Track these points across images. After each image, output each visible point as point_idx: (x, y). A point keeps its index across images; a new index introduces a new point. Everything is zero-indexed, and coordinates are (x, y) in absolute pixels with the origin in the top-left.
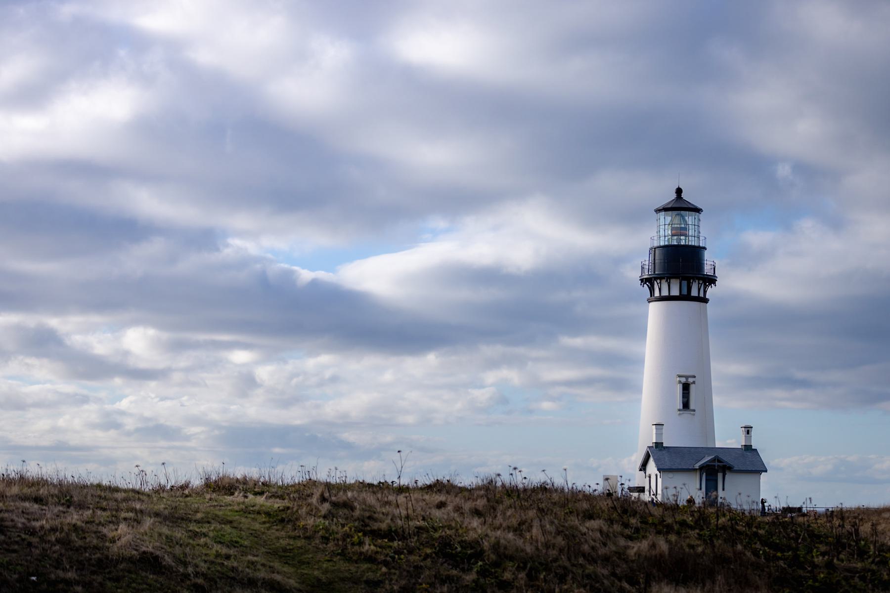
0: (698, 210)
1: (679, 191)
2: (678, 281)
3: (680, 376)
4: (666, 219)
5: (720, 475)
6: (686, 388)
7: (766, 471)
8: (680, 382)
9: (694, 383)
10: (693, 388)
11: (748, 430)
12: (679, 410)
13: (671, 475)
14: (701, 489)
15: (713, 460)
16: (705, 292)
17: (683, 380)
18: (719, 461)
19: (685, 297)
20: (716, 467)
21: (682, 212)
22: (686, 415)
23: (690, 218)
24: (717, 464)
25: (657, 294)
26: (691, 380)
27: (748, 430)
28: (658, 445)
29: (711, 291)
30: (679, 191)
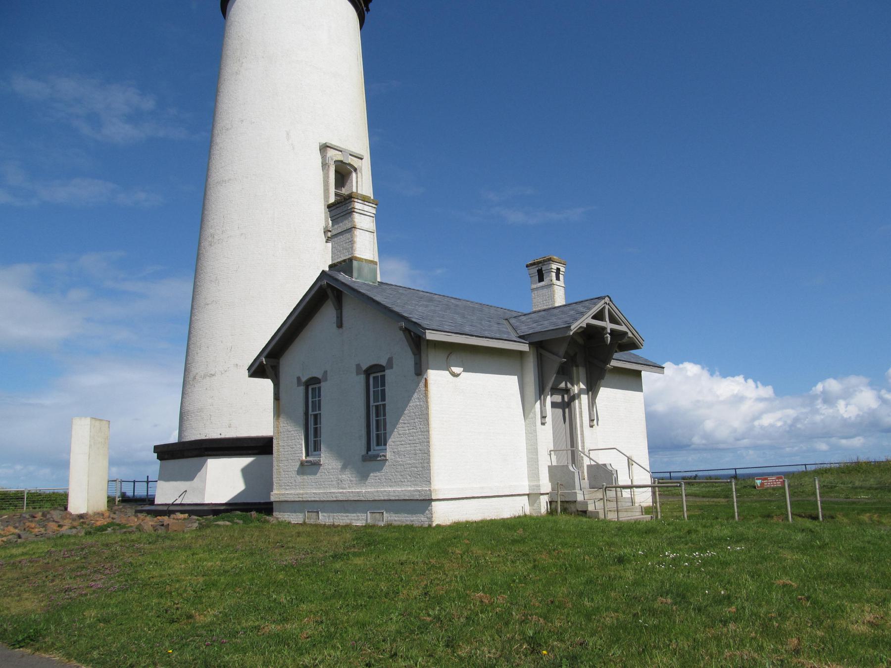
3: (324, 148)
14: (544, 417)
15: (599, 316)
24: (609, 326)
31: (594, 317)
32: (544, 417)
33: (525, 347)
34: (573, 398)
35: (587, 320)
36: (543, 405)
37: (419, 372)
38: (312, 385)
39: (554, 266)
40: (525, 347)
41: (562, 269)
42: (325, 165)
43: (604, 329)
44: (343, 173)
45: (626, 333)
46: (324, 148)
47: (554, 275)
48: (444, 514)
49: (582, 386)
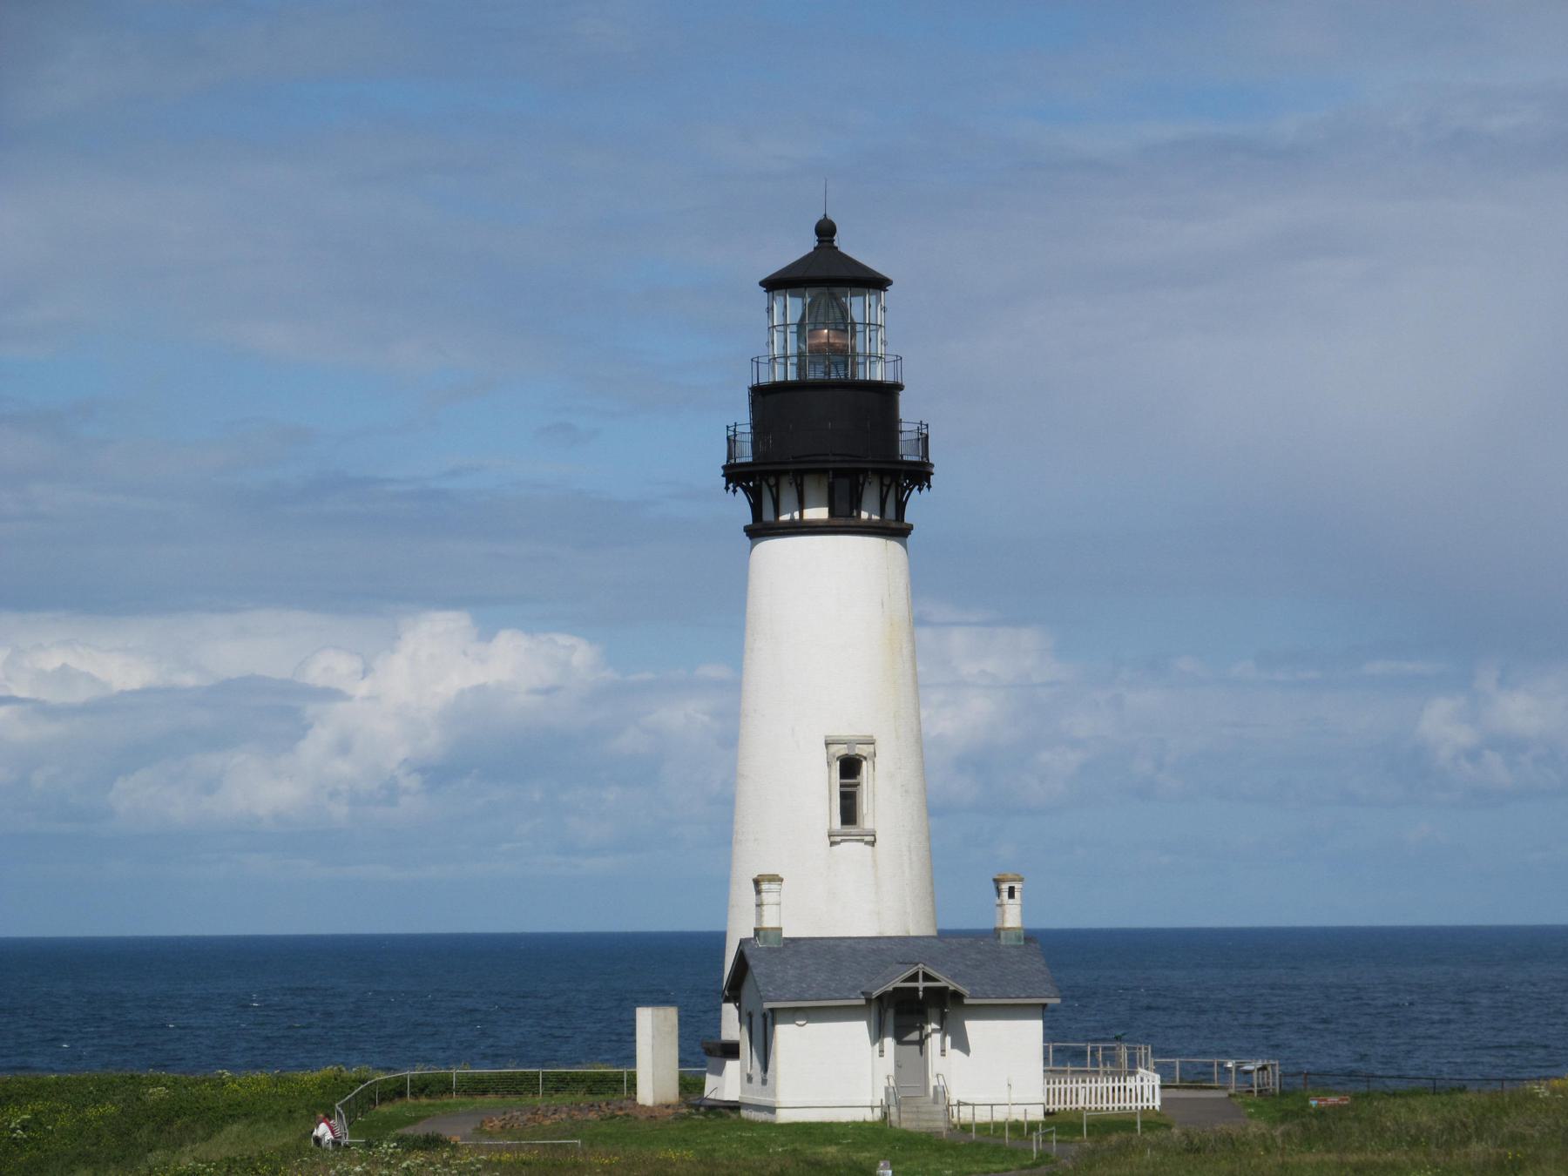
0: (878, 283)
1: (826, 231)
2: (825, 482)
4: (793, 307)
6: (850, 767)
15: (914, 978)
16: (901, 507)
17: (842, 750)
18: (927, 977)
19: (842, 523)
21: (837, 290)
22: (852, 850)
23: (858, 306)
24: (921, 985)
25: (768, 515)
26: (862, 750)
29: (918, 505)
30: (826, 231)
31: (906, 980)
33: (863, 1002)
34: (928, 1036)
35: (897, 983)
36: (882, 1044)
37: (773, 1024)
38: (750, 1015)
39: (1005, 887)
40: (863, 1002)
41: (1017, 886)
42: (829, 764)
43: (917, 989)
44: (850, 767)
45: (946, 988)
46: (827, 744)
47: (1005, 895)
48: (783, 1117)
49: (934, 1026)
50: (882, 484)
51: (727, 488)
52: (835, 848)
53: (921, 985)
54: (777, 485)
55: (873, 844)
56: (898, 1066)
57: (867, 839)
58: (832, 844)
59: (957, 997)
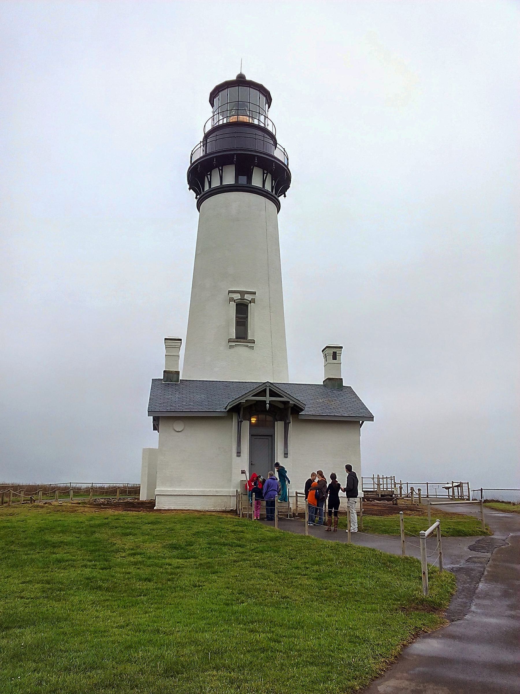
3: (230, 292)
5: (279, 426)
7: (371, 418)
8: (232, 300)
9: (253, 301)
10: (251, 306)
11: (333, 353)
12: (230, 341)
13: (179, 426)
14: (239, 454)
15: (262, 393)
17: (237, 296)
18: (273, 394)
20: (267, 411)
22: (242, 351)
24: (268, 399)
26: (247, 297)
27: (333, 353)
28: (171, 377)
32: (239, 454)
39: (331, 351)
50: (264, 173)
51: (190, 189)
52: (232, 350)
53: (268, 399)
54: (211, 175)
55: (252, 348)
56: (251, 464)
57: (249, 345)
58: (231, 347)
59: (296, 410)
